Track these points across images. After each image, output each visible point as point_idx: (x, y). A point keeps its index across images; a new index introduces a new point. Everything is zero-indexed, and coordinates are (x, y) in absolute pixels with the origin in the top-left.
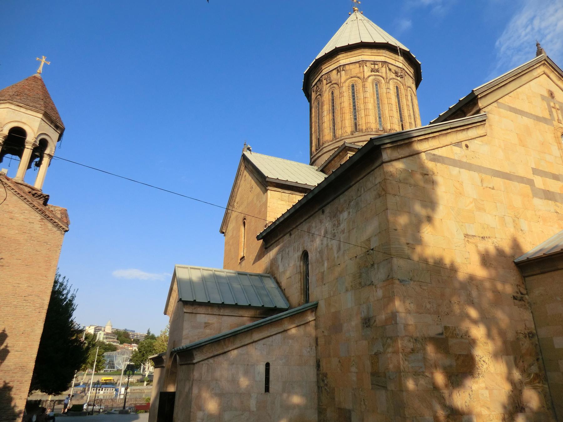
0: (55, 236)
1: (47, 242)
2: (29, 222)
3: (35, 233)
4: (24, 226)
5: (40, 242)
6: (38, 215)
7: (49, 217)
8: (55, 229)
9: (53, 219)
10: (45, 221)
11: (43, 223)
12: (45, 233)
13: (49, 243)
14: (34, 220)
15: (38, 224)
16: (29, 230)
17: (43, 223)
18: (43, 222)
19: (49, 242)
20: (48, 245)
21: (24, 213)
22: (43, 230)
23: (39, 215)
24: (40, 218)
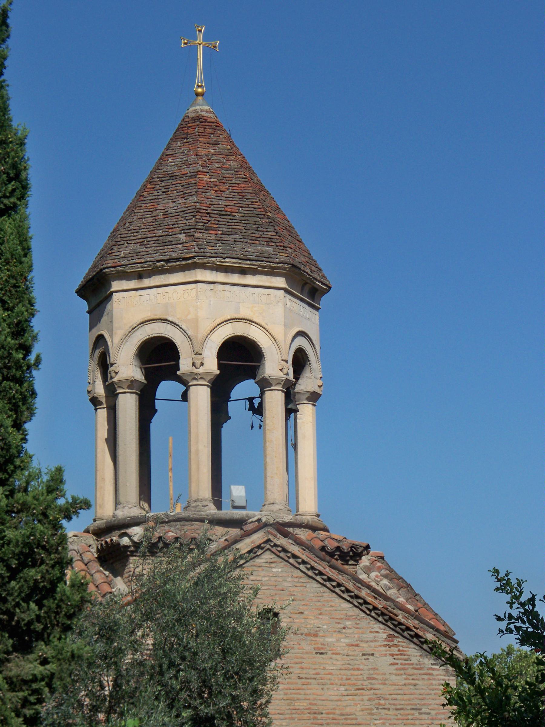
0: (434, 682)
1: (418, 707)
2: (363, 655)
3: (385, 684)
4: (354, 669)
5: (402, 709)
6: (377, 626)
7: (408, 629)
8: (428, 661)
9: (420, 633)
10: (398, 640)
11: (395, 650)
12: (406, 679)
13: (424, 710)
14: (372, 644)
15: (386, 655)
16: (369, 678)
17: (397, 649)
18: (397, 646)
19: (424, 705)
20: (424, 716)
21: (344, 628)
22: (402, 672)
23: (382, 626)
24: (385, 636)
